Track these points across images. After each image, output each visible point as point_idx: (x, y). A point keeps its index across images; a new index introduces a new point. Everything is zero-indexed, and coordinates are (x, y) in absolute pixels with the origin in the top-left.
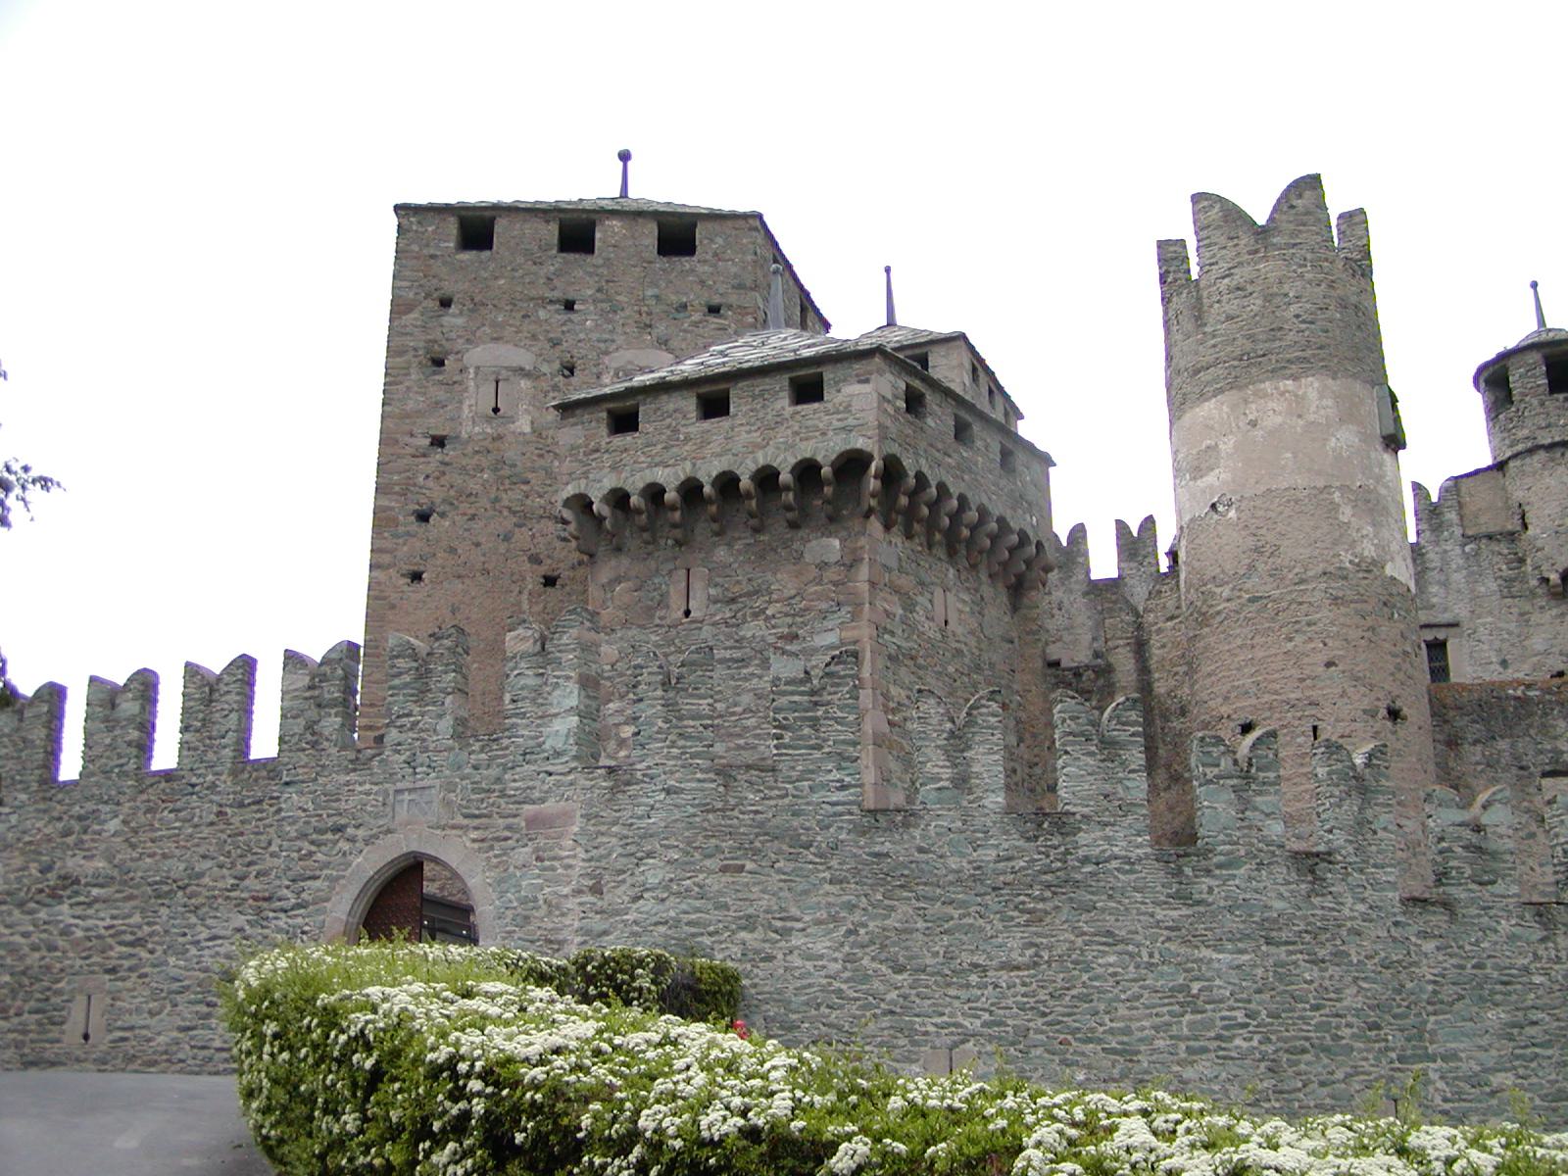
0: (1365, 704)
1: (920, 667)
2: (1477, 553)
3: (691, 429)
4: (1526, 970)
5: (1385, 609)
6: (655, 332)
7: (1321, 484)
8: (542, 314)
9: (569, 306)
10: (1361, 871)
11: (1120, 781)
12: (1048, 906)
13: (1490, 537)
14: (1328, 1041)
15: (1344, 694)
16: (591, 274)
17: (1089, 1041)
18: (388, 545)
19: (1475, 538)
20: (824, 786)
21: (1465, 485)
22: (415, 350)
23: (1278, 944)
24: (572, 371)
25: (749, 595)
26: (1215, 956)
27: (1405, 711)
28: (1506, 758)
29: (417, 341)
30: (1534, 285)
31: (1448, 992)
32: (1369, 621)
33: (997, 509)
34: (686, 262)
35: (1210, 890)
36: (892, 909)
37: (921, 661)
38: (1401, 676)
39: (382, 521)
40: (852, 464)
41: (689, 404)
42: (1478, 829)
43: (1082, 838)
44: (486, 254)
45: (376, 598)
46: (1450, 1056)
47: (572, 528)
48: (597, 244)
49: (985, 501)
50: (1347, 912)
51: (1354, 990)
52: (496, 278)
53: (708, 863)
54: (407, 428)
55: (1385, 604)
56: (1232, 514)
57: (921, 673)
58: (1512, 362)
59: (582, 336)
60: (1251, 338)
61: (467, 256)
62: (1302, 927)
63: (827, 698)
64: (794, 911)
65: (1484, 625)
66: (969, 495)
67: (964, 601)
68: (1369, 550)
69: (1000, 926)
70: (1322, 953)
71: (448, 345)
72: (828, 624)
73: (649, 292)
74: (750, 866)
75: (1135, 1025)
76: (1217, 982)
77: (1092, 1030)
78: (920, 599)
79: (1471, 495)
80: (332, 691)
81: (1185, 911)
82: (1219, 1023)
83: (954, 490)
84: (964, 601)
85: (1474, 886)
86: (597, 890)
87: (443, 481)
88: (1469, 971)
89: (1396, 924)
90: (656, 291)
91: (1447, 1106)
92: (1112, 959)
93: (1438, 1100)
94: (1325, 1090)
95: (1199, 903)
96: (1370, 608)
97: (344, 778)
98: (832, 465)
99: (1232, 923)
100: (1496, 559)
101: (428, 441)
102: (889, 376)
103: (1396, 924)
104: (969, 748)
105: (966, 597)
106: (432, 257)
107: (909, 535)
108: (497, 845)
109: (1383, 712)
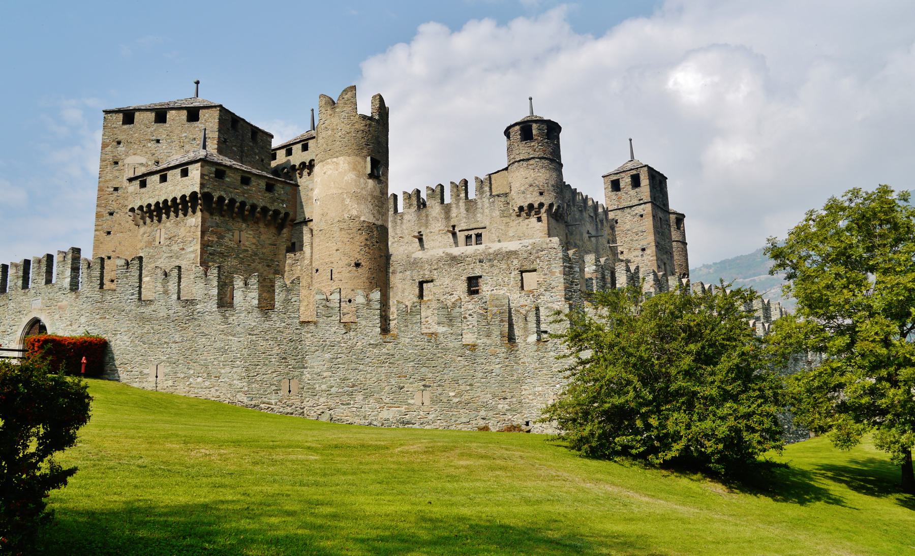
0: (347, 262)
1: (225, 256)
2: (493, 202)
3: (158, 186)
4: (339, 342)
5: (360, 231)
6: (184, 148)
7: (340, 191)
8: (149, 145)
9: (158, 141)
10: (285, 314)
11: (209, 290)
12: (187, 325)
13: (498, 196)
14: (267, 362)
15: (340, 259)
16: (165, 130)
17: (194, 363)
18: (100, 223)
19: (494, 196)
20: (128, 294)
21: (493, 176)
22: (109, 159)
23: (252, 335)
24: (158, 163)
25: (174, 237)
26: (233, 338)
27: (363, 263)
28: (409, 277)
29: (110, 157)
30: (531, 99)
31: (313, 349)
32: (351, 236)
33: (261, 203)
34: (196, 124)
35: (233, 320)
36: (145, 327)
37: (225, 254)
38: (363, 252)
39: (99, 216)
40: (194, 194)
41: (157, 177)
42: (327, 300)
43: (198, 306)
44: (132, 125)
45: (96, 240)
46: (312, 367)
47: (131, 218)
48: (167, 119)
49: (255, 202)
50: (277, 326)
51: (277, 348)
52: (135, 133)
53: (96, 316)
54: (106, 185)
55: (359, 230)
56: (319, 203)
57: (226, 258)
58: (511, 130)
59: (162, 151)
60: (327, 145)
61: (126, 127)
62: (261, 330)
63: (130, 270)
64: (119, 329)
65: (494, 227)
66: (247, 201)
67: (250, 234)
68: (354, 213)
69: (173, 331)
70: (267, 338)
71: (119, 157)
72: (192, 245)
73: (183, 135)
74: (108, 317)
75: (208, 358)
76: (233, 346)
77: (197, 359)
78: (227, 235)
79: (495, 180)
80: (21, 273)
81: (226, 326)
82: (233, 357)
83: (239, 199)
84: (250, 234)
85: (325, 318)
86: (71, 325)
87: (117, 202)
88: (321, 342)
89: (297, 329)
90: (185, 134)
91: (309, 382)
92: (203, 340)
93: (306, 380)
94: (264, 376)
95: (229, 324)
96: (352, 231)
97: (22, 298)
98: (190, 196)
99: (238, 329)
100: (500, 203)
101: (113, 189)
102: (207, 167)
103: (297, 329)
104: (168, 282)
105: (251, 233)
106: (115, 128)
107: (223, 216)
108: (53, 314)
109: (353, 264)
